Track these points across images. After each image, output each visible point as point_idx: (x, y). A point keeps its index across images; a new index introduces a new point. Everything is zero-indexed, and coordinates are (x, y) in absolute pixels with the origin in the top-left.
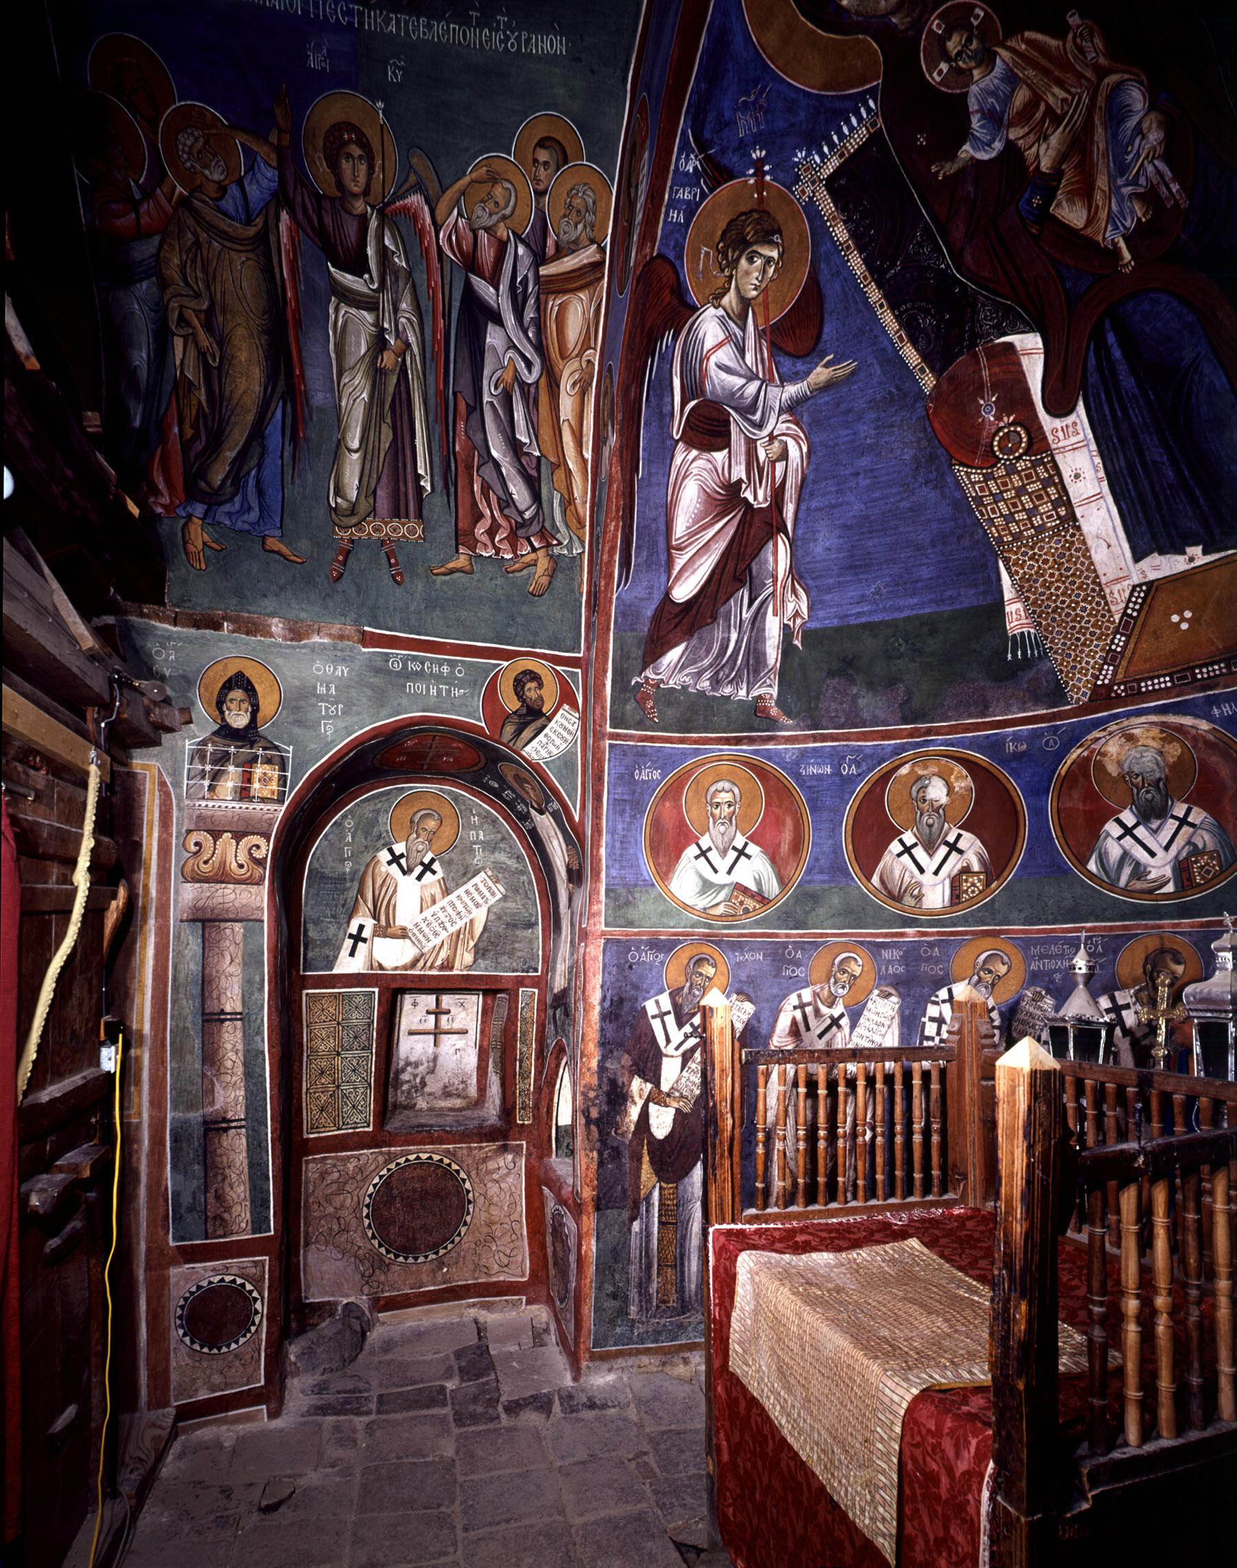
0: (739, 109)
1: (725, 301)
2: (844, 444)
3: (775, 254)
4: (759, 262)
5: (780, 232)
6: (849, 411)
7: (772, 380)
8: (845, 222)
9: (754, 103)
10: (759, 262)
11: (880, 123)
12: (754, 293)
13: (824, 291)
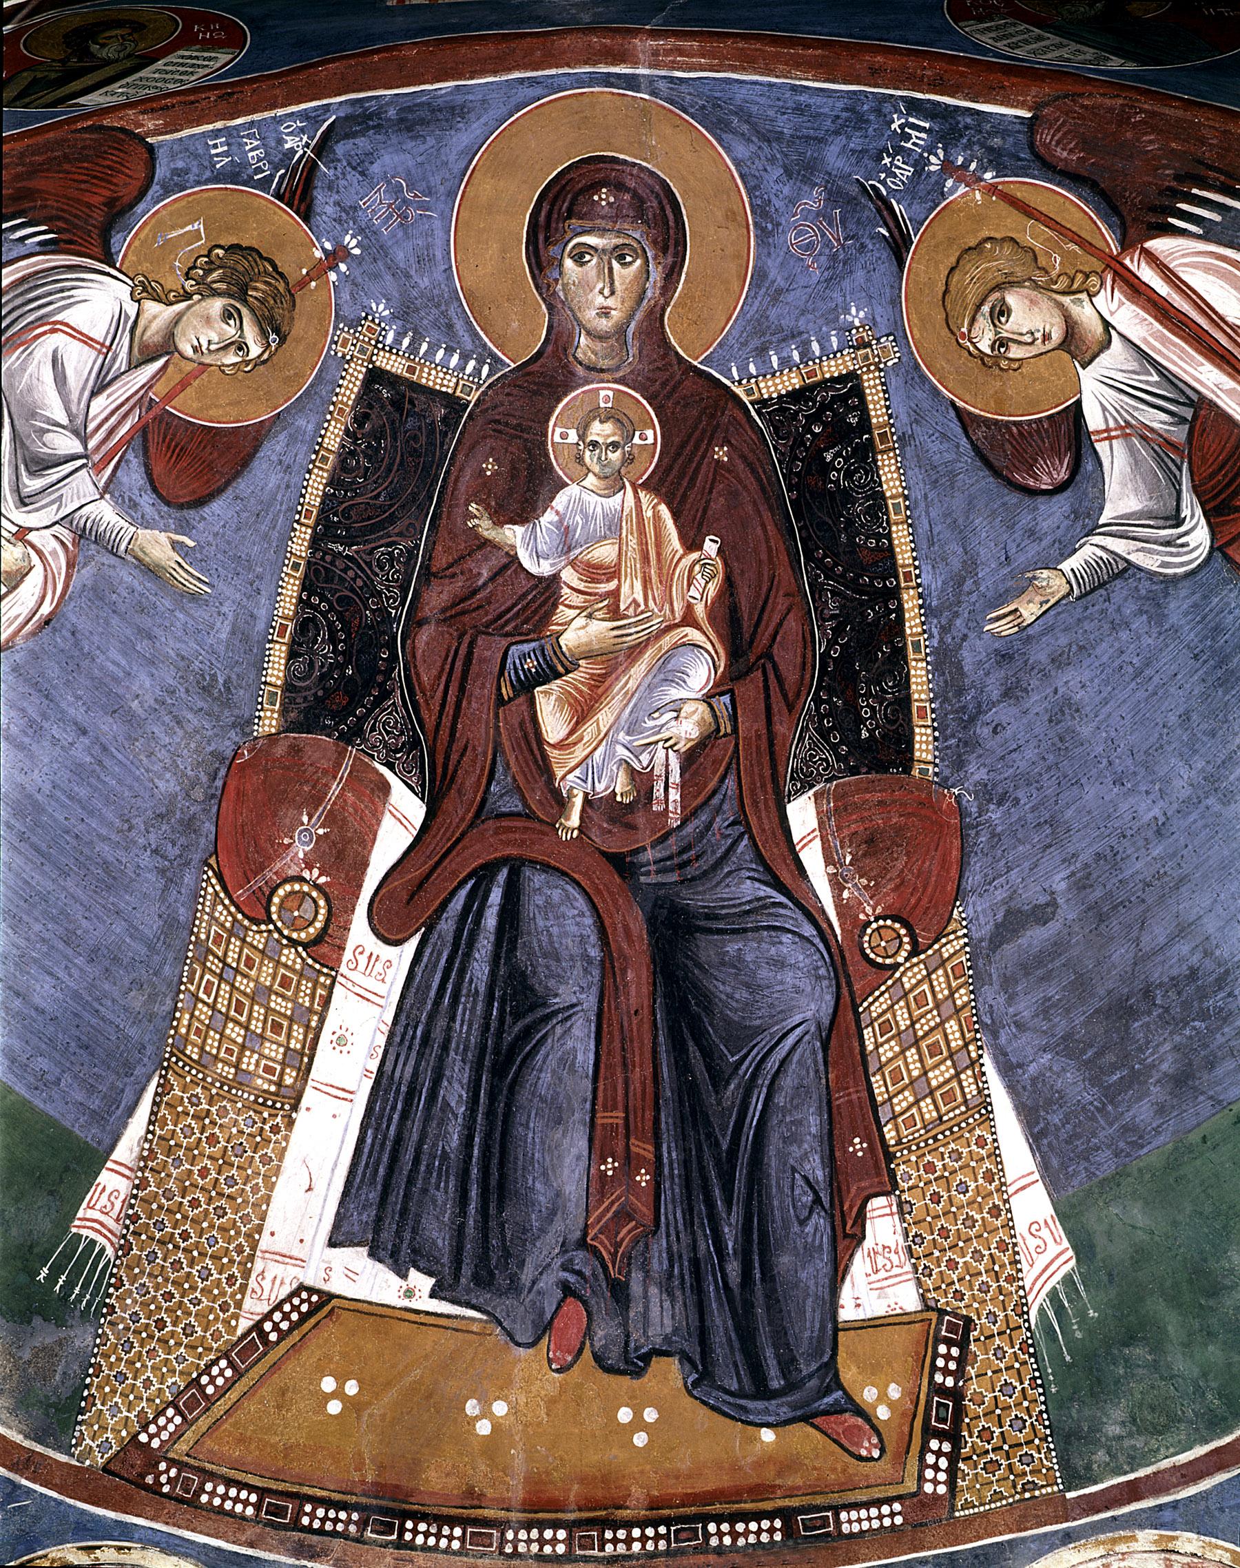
0: (389, 183)
1: (151, 307)
2: (102, 668)
3: (255, 350)
4: (231, 330)
5: (283, 339)
6: (150, 637)
7: (99, 468)
8: (347, 432)
9: (405, 201)
10: (231, 330)
11: (473, 398)
12: (189, 352)
13: (255, 463)
